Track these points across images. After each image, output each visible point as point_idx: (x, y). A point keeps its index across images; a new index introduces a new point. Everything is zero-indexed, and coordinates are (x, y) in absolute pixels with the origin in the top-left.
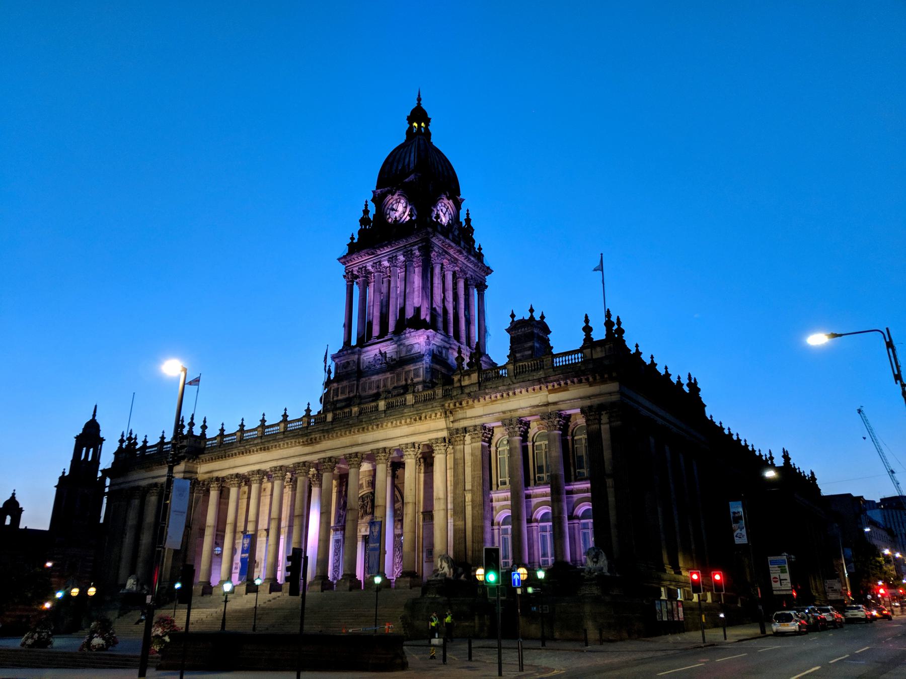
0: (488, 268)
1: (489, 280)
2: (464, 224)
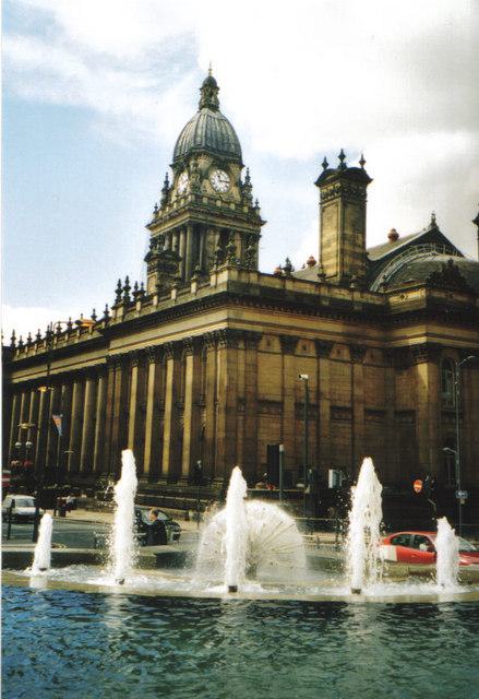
0: (260, 221)
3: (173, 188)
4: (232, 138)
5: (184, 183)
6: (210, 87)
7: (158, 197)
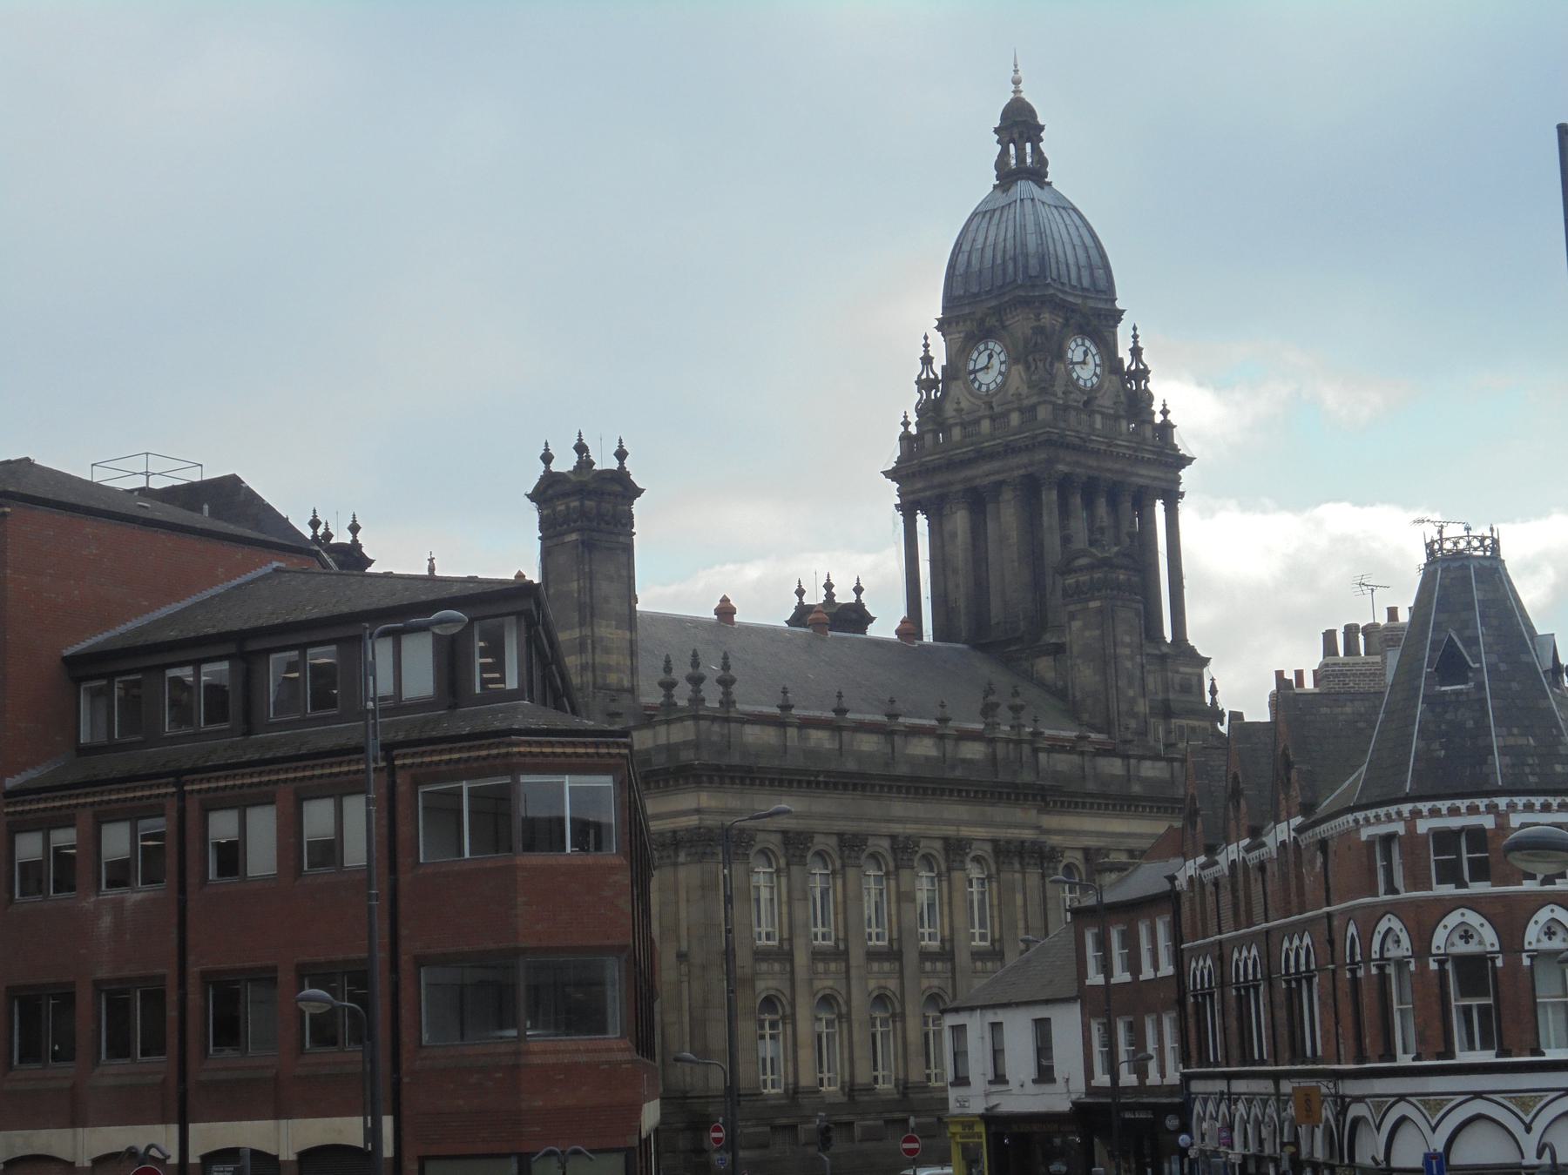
1: (1187, 477)
2: (1126, 363)
4: (1093, 252)
5: (991, 368)
7: (908, 401)
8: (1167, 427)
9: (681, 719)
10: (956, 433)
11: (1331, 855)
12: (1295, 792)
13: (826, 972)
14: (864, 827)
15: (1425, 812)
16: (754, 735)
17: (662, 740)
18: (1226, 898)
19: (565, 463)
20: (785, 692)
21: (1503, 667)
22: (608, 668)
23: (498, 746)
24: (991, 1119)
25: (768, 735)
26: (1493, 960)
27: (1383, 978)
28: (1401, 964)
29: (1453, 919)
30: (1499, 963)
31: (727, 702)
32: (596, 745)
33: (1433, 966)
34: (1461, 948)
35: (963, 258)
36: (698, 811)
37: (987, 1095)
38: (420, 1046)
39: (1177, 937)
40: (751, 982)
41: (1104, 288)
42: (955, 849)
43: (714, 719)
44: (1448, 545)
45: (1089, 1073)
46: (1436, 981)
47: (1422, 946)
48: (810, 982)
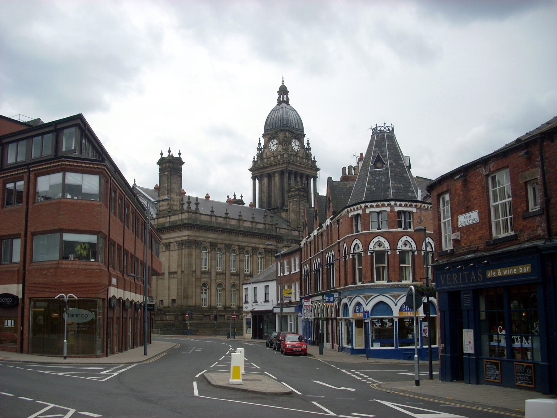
3: (266, 146)
4: (299, 121)
5: (274, 146)
6: (283, 91)
7: (255, 153)
8: (315, 161)
9: (185, 213)
10: (266, 160)
11: (340, 225)
12: (331, 209)
13: (220, 278)
14: (231, 243)
15: (369, 206)
16: (203, 218)
17: (180, 218)
18: (313, 246)
19: (166, 155)
20: (212, 208)
21: (394, 164)
22: (174, 205)
23: (59, 162)
24: (253, 312)
25: (208, 218)
26: (388, 252)
27: (354, 259)
28: (359, 254)
29: (376, 240)
30: (389, 253)
31: (197, 209)
32: (93, 164)
33: (369, 254)
34: (378, 249)
35: (269, 121)
36: (188, 235)
37: (253, 306)
38: (32, 262)
39: (300, 261)
40: (200, 279)
41: (302, 130)
42: (255, 249)
43: (193, 213)
44: (379, 129)
45: (278, 300)
46: (369, 259)
47: (366, 249)
48: (215, 280)
